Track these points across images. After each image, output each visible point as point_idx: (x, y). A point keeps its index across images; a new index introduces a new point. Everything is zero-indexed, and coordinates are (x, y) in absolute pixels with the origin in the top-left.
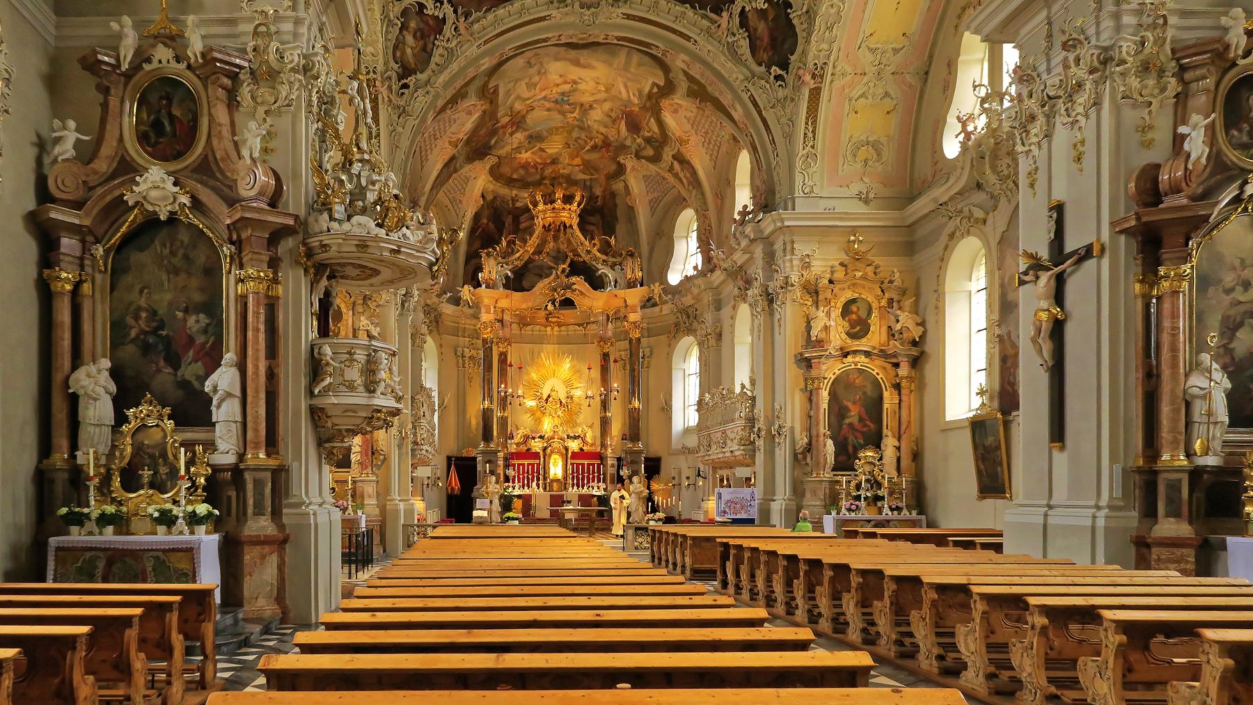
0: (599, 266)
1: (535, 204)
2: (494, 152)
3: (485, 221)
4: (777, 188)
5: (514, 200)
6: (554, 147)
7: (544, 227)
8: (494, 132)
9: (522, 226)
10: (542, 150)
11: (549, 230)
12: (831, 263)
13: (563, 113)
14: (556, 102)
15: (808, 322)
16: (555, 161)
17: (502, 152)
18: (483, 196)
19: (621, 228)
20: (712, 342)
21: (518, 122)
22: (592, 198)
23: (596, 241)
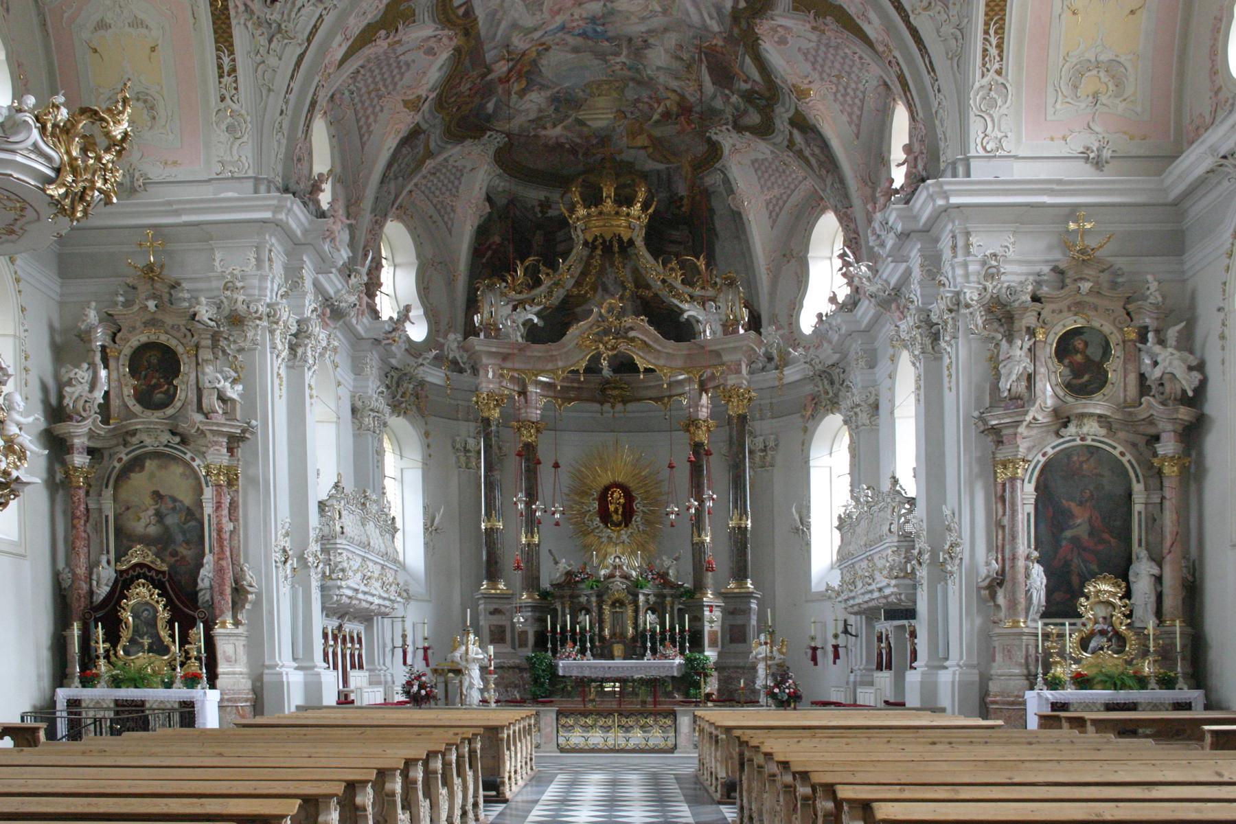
0: (685, 306)
1: (572, 210)
2: (498, 125)
3: (497, 239)
4: (942, 145)
5: (545, 205)
6: (600, 116)
7: (586, 243)
8: (487, 91)
9: (561, 248)
10: (581, 123)
11: (594, 248)
12: (1037, 268)
13: (602, 56)
14: (584, 35)
15: (996, 368)
16: (604, 139)
17: (515, 125)
18: (489, 199)
19: (723, 247)
20: (864, 417)
21: (526, 71)
22: (674, 200)
23: (674, 264)
